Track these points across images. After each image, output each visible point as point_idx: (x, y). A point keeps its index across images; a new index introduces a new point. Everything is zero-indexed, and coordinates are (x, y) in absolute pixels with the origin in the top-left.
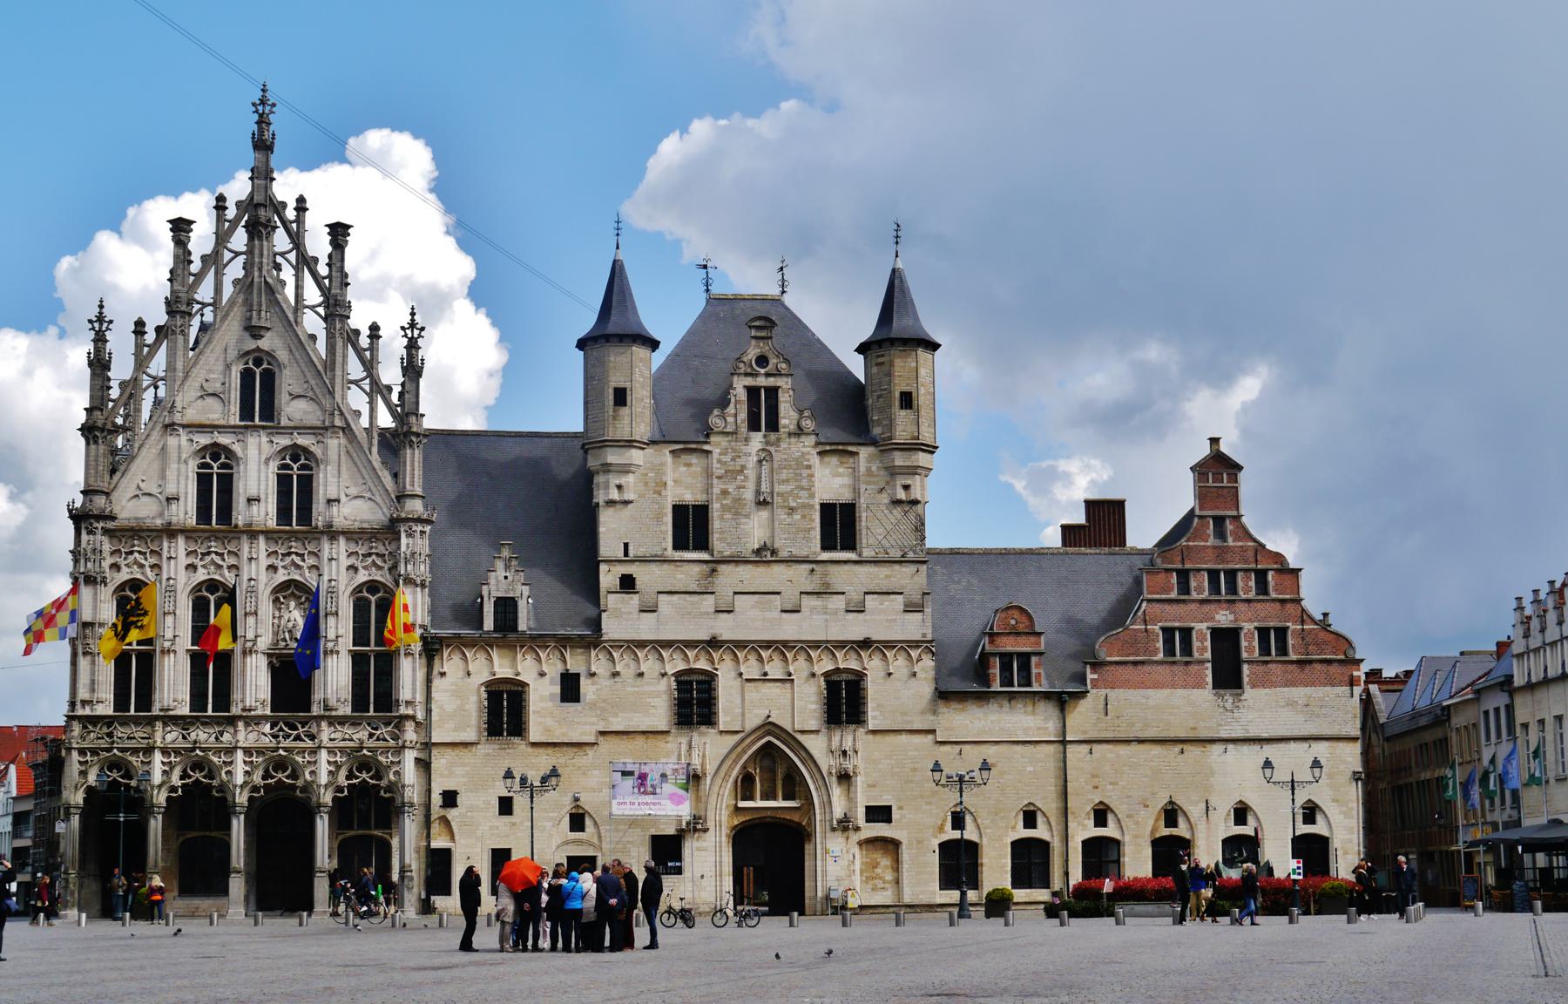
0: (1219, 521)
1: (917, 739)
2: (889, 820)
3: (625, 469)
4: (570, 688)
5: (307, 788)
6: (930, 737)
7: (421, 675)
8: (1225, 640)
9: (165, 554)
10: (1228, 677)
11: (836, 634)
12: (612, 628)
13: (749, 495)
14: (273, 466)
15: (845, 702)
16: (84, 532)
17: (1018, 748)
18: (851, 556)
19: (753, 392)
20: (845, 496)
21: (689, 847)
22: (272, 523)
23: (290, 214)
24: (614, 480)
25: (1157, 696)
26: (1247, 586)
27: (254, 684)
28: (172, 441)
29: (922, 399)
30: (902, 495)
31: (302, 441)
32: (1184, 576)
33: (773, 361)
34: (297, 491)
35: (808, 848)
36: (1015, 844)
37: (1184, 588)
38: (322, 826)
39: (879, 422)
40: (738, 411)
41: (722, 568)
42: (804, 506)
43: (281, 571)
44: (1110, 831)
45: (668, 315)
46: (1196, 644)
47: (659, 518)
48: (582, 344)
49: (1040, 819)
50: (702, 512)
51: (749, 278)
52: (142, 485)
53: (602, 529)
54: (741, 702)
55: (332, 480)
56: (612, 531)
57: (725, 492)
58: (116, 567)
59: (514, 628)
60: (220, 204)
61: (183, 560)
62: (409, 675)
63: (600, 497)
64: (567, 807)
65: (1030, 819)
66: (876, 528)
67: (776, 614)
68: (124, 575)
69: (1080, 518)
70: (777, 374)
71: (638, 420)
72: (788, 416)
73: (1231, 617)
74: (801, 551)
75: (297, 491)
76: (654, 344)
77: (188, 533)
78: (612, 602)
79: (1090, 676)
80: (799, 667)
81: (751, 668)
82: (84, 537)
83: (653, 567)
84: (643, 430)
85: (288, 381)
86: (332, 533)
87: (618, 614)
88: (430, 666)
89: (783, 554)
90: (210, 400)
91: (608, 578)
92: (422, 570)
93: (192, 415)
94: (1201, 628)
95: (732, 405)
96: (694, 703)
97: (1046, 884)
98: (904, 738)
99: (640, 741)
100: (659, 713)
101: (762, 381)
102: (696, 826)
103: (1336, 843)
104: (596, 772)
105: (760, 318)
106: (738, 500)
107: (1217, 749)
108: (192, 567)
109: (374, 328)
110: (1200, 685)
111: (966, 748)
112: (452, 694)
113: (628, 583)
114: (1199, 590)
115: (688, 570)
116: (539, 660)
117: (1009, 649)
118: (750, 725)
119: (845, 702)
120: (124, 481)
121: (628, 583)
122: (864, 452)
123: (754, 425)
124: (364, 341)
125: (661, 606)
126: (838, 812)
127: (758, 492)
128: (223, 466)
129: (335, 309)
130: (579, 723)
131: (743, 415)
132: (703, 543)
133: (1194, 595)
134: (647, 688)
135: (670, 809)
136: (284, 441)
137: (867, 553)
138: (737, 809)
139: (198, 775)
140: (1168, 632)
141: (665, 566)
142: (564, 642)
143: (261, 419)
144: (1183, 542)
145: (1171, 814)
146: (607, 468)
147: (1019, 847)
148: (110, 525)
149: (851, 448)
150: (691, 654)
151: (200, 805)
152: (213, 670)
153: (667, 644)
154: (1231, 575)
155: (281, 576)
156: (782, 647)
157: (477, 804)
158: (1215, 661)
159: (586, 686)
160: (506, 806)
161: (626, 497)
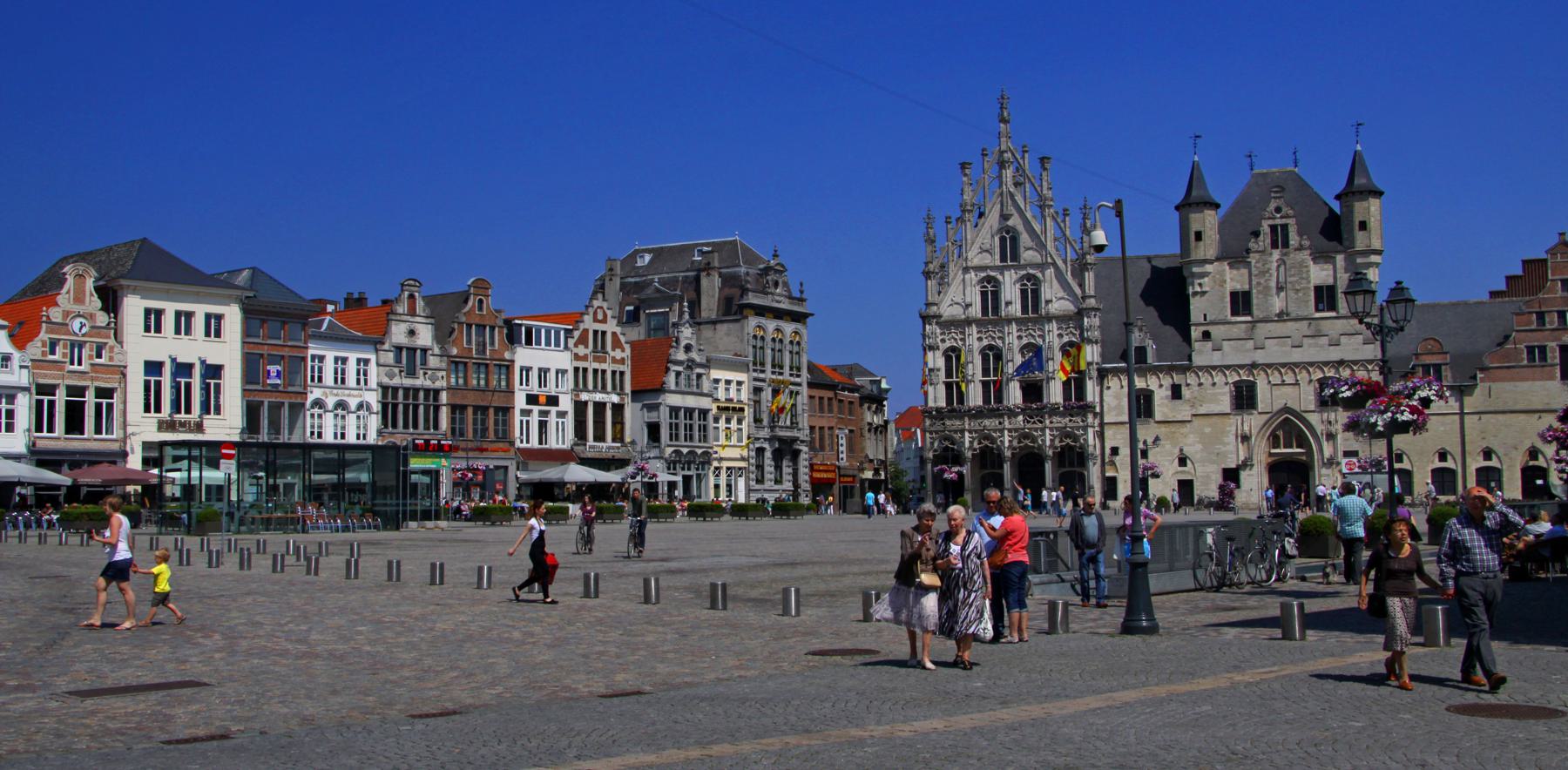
3: (1203, 275)
4: (1176, 392)
5: (1040, 447)
7: (1098, 389)
12: (1198, 360)
13: (1273, 284)
18: (1333, 314)
19: (1273, 228)
20: (1330, 281)
21: (1244, 475)
22: (1019, 314)
27: (1014, 395)
32: (1541, 316)
33: (1285, 210)
34: (1031, 297)
38: (1048, 466)
40: (1265, 240)
44: (1494, 463)
45: (1225, 188)
46: (1549, 355)
47: (1222, 299)
48: (1177, 208)
51: (1273, 165)
54: (1269, 396)
56: (1197, 308)
58: (943, 341)
59: (1145, 362)
61: (976, 336)
62: (1091, 389)
63: (1191, 290)
64: (1177, 452)
65: (1443, 456)
68: (948, 344)
69: (1519, 272)
70: (1287, 216)
71: (1208, 247)
72: (1294, 239)
74: (1305, 314)
75: (1031, 297)
76: (1217, 206)
77: (978, 322)
78: (1196, 345)
79: (1479, 376)
83: (1221, 327)
84: (1211, 253)
85: (1025, 239)
86: (1049, 318)
87: (1201, 352)
88: (1101, 384)
89: (1293, 315)
91: (1195, 333)
92: (1097, 334)
93: (976, 262)
94: (1552, 344)
96: (1244, 398)
97: (1454, 492)
100: (1225, 404)
101: (1278, 222)
102: (1246, 464)
106: (1267, 288)
108: (980, 339)
110: (1552, 378)
112: (1113, 398)
113: (1206, 336)
114: (1552, 323)
118: (1276, 408)
121: (1206, 336)
123: (1274, 245)
125: (1223, 347)
130: (1182, 411)
131: (1268, 241)
132: (1247, 310)
133: (1548, 326)
135: (1233, 455)
138: (1271, 455)
140: (1530, 350)
142: (1170, 370)
147: (1436, 473)
151: (988, 458)
152: (994, 390)
153: (1228, 367)
155: (1025, 341)
156: (1292, 366)
159: (1185, 392)
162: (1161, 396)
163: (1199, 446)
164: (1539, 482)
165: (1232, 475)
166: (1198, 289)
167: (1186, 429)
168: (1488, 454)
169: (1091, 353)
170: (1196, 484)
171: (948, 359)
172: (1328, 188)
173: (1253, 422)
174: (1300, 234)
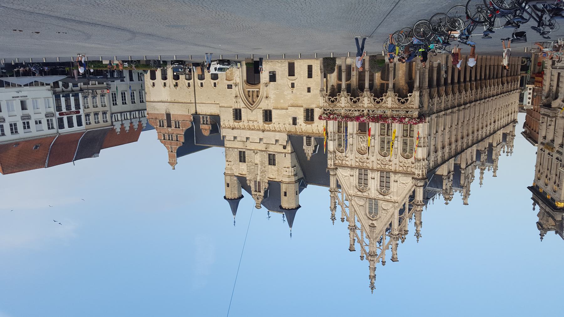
1: (223, 105)
2: (228, 85)
4: (295, 121)
8: (169, 126)
9: (398, 166)
10: (168, 115)
13: (259, 166)
15: (237, 115)
19: (260, 192)
21: (268, 79)
23: (365, 255)
24: (287, 174)
25: (180, 113)
26: (167, 137)
31: (359, 193)
35: (245, 78)
36: (204, 79)
41: (264, 149)
42: (248, 162)
43: (366, 158)
46: (174, 124)
47: (278, 162)
57: (265, 167)
59: (307, 137)
60: (384, 263)
65: (202, 84)
66: (235, 155)
67: (251, 137)
68: (410, 160)
80: (246, 124)
82: (421, 173)
89: (252, 151)
91: (289, 149)
93: (391, 205)
94: (173, 128)
96: (268, 116)
98: (226, 105)
99: (279, 106)
101: (258, 194)
106: (262, 165)
107: (169, 100)
109: (343, 220)
113: (285, 147)
115: (273, 149)
116: (301, 129)
119: (237, 115)
120: (410, 188)
121: (285, 147)
122: (237, 174)
124: (345, 217)
129: (353, 228)
136: (365, 194)
137: (236, 150)
139: (378, 100)
140: (179, 128)
144: (178, 147)
145: (176, 85)
146: (289, 177)
150: (268, 129)
156: (250, 129)
157: (316, 91)
158: (171, 120)
159: (291, 121)
160: (309, 90)
161: (285, 169)
162: (301, 120)
164: (175, 74)
165: (273, 77)
166: (287, 169)
167: (291, 102)
168: (189, 85)
169: (331, 146)
170: (287, 74)
172: (248, 201)
173: (265, 105)
174: (250, 186)
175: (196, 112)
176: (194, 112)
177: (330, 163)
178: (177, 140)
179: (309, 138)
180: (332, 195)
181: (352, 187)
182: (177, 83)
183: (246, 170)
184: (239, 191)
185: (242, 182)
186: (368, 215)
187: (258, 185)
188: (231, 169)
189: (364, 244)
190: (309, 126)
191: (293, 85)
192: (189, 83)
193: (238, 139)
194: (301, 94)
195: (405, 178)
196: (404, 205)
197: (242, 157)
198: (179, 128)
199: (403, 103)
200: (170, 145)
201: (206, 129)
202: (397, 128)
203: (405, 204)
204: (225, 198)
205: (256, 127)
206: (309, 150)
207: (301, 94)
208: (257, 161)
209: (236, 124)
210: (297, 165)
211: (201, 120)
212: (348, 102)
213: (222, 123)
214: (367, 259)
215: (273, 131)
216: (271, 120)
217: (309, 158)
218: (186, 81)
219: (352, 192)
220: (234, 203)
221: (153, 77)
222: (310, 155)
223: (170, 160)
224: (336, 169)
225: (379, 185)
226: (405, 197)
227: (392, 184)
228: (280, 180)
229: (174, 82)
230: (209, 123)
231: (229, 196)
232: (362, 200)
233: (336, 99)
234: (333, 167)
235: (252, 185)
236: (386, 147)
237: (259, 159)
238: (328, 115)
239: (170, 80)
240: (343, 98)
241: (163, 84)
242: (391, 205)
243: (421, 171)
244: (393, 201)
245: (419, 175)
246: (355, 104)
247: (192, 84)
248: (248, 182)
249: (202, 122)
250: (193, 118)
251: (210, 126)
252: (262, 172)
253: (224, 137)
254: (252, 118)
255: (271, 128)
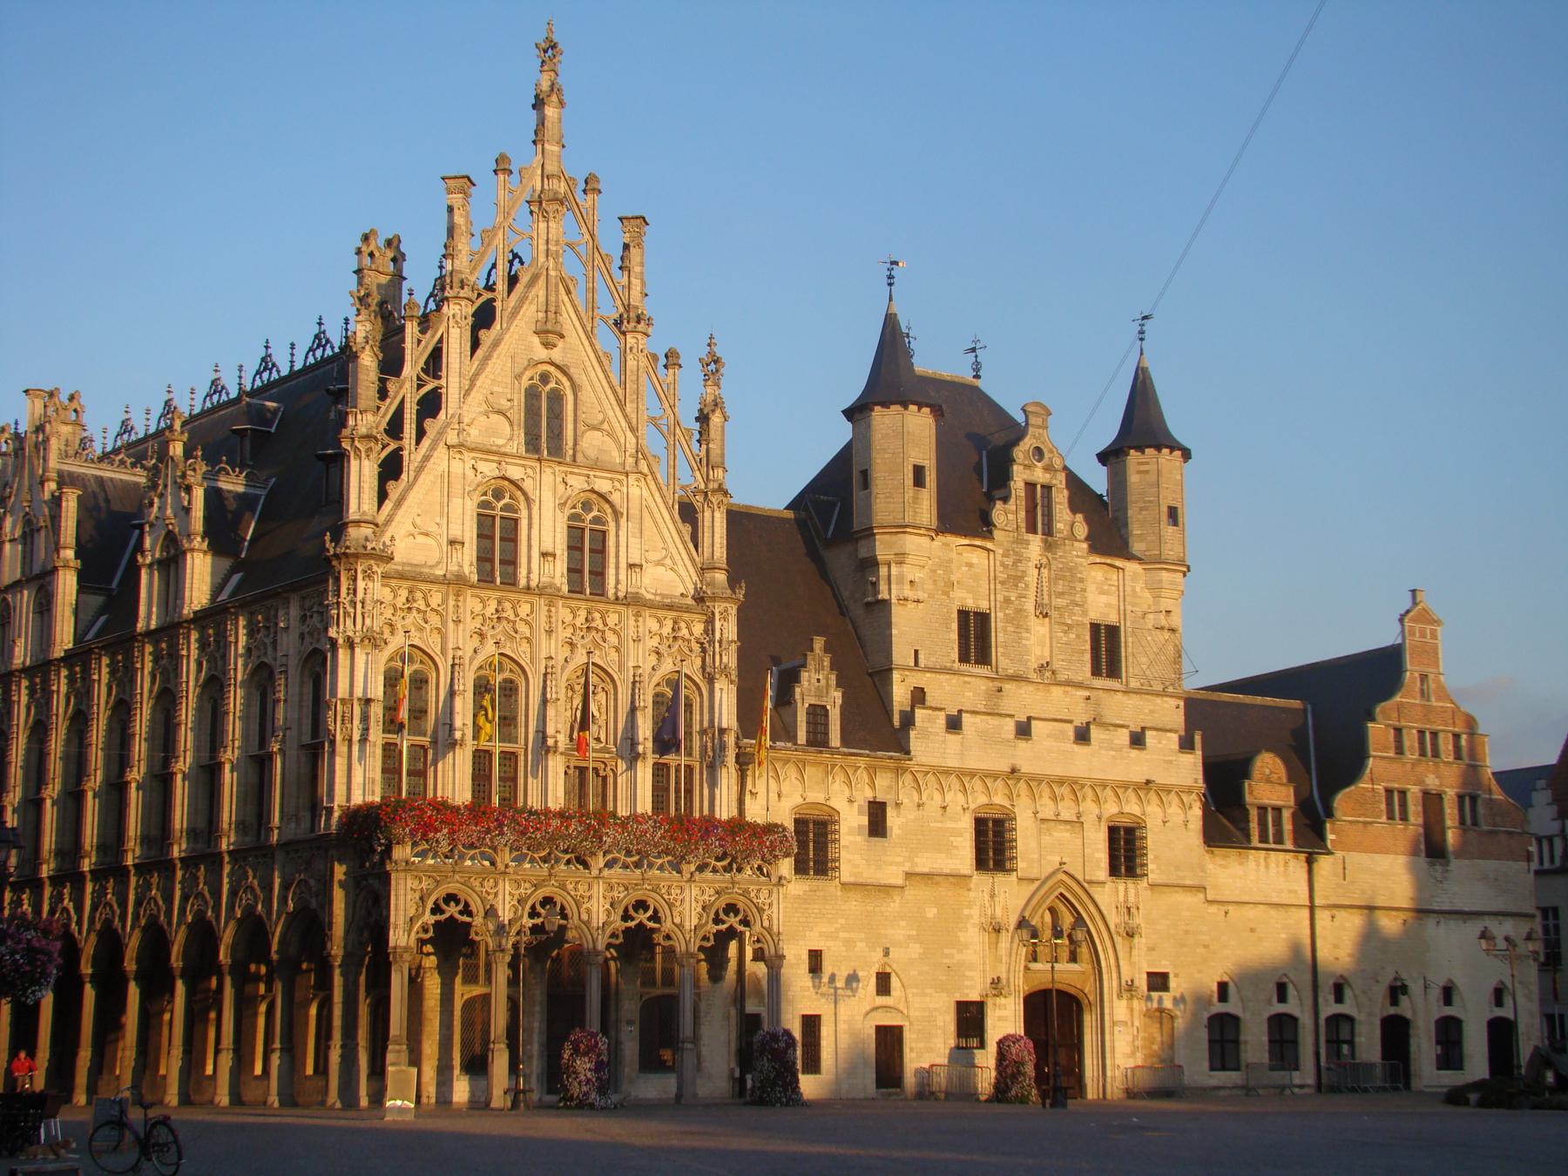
0: (1424, 677)
6: (1201, 896)
9: (451, 616)
11: (1118, 773)
13: (1030, 606)
14: (568, 512)
15: (1125, 850)
16: (360, 576)
17: (1273, 912)
19: (1030, 486)
24: (910, 572)
28: (457, 466)
29: (1186, 516)
30: (1163, 623)
31: (603, 485)
32: (1398, 731)
35: (1089, 1021)
37: (1399, 750)
39: (1141, 538)
49: (1291, 992)
50: (983, 619)
52: (418, 520)
53: (894, 632)
54: (1034, 848)
55: (634, 541)
57: (1007, 600)
66: (1137, 656)
68: (396, 642)
73: (1437, 782)
81: (1047, 809)
82: (361, 584)
89: (1062, 677)
90: (495, 417)
93: (474, 435)
94: (1414, 791)
95: (1012, 500)
96: (993, 844)
103: (1521, 1028)
104: (903, 923)
105: (1038, 404)
106: (1019, 611)
111: (1231, 908)
113: (919, 696)
117: (1266, 802)
119: (1125, 850)
121: (919, 696)
122: (1132, 567)
123: (1032, 529)
126: (1125, 977)
127: (1037, 605)
128: (506, 508)
131: (1022, 514)
132: (984, 658)
134: (949, 825)
136: (577, 482)
137: (1134, 684)
140: (1389, 792)
141: (955, 680)
143: (549, 453)
144: (1397, 698)
146: (901, 559)
148: (391, 567)
149: (1118, 563)
154: (1434, 734)
156: (1074, 785)
159: (893, 819)
161: (921, 595)
162: (852, 821)
163: (915, 950)
166: (908, 592)
167: (894, 904)
171: (392, 679)
173: (1007, 896)
175: (1310, 862)
176: (1324, 864)
177: (728, 628)
178: (1398, 731)
179: (818, 739)
180: (719, 473)
181: (634, 511)
182: (1394, 1002)
183: (1091, 588)
184: (1118, 482)
185: (1109, 530)
186: (564, 380)
187: (1038, 517)
188: (1155, 589)
189: (582, 250)
190: (816, 796)
191: (884, 983)
192: (1339, 998)
193: (1123, 737)
194: (849, 943)
195: (418, 558)
196: (421, 434)
197: (1106, 649)
198: (1389, 792)
199: (451, 898)
200: (1429, 709)
201: (1270, 784)
202: (454, 781)
203: (418, 442)
204: (1186, 454)
205: (1046, 792)
206: (818, 685)
207: (849, 943)
208: (1039, 630)
209: (1133, 808)
210: (857, 611)
211: (1287, 826)
212: (670, 905)
213: (1197, 811)
214: (571, 182)
215: (972, 774)
216: (980, 823)
217: (819, 643)
218: (1352, 1012)
219: (635, 492)
220: (1142, 427)
221: (1501, 1033)
222: (811, 664)
223: (1434, 635)
224: (700, 599)
225: (524, 524)
226: (420, 470)
227: (469, 533)
228: (940, 539)
229: (1405, 1008)
230: (1254, 814)
231: (1167, 460)
232: (592, 453)
233: (717, 921)
234: (718, 608)
235: (1063, 515)
236: (499, 694)
237: (1029, 641)
238: (742, 842)
239: (1423, 1012)
240: (691, 921)
241: (1456, 999)
242: (474, 432)
243: (360, 595)
244: (467, 455)
245: (369, 575)
246: (638, 895)
247: (1327, 996)
248: (1082, 530)
249: (1286, 814)
250: (1321, 836)
251: (1248, 798)
252: (1016, 579)
253: (1186, 744)
254: (1062, 834)
255: (977, 782)
